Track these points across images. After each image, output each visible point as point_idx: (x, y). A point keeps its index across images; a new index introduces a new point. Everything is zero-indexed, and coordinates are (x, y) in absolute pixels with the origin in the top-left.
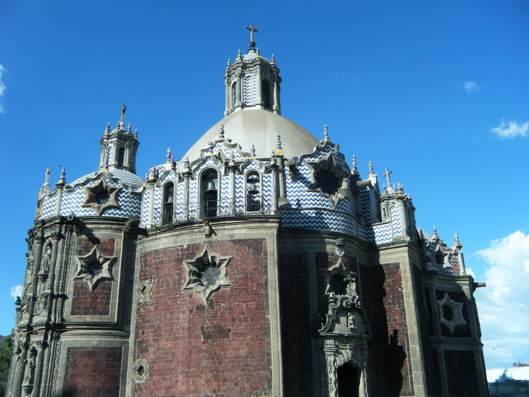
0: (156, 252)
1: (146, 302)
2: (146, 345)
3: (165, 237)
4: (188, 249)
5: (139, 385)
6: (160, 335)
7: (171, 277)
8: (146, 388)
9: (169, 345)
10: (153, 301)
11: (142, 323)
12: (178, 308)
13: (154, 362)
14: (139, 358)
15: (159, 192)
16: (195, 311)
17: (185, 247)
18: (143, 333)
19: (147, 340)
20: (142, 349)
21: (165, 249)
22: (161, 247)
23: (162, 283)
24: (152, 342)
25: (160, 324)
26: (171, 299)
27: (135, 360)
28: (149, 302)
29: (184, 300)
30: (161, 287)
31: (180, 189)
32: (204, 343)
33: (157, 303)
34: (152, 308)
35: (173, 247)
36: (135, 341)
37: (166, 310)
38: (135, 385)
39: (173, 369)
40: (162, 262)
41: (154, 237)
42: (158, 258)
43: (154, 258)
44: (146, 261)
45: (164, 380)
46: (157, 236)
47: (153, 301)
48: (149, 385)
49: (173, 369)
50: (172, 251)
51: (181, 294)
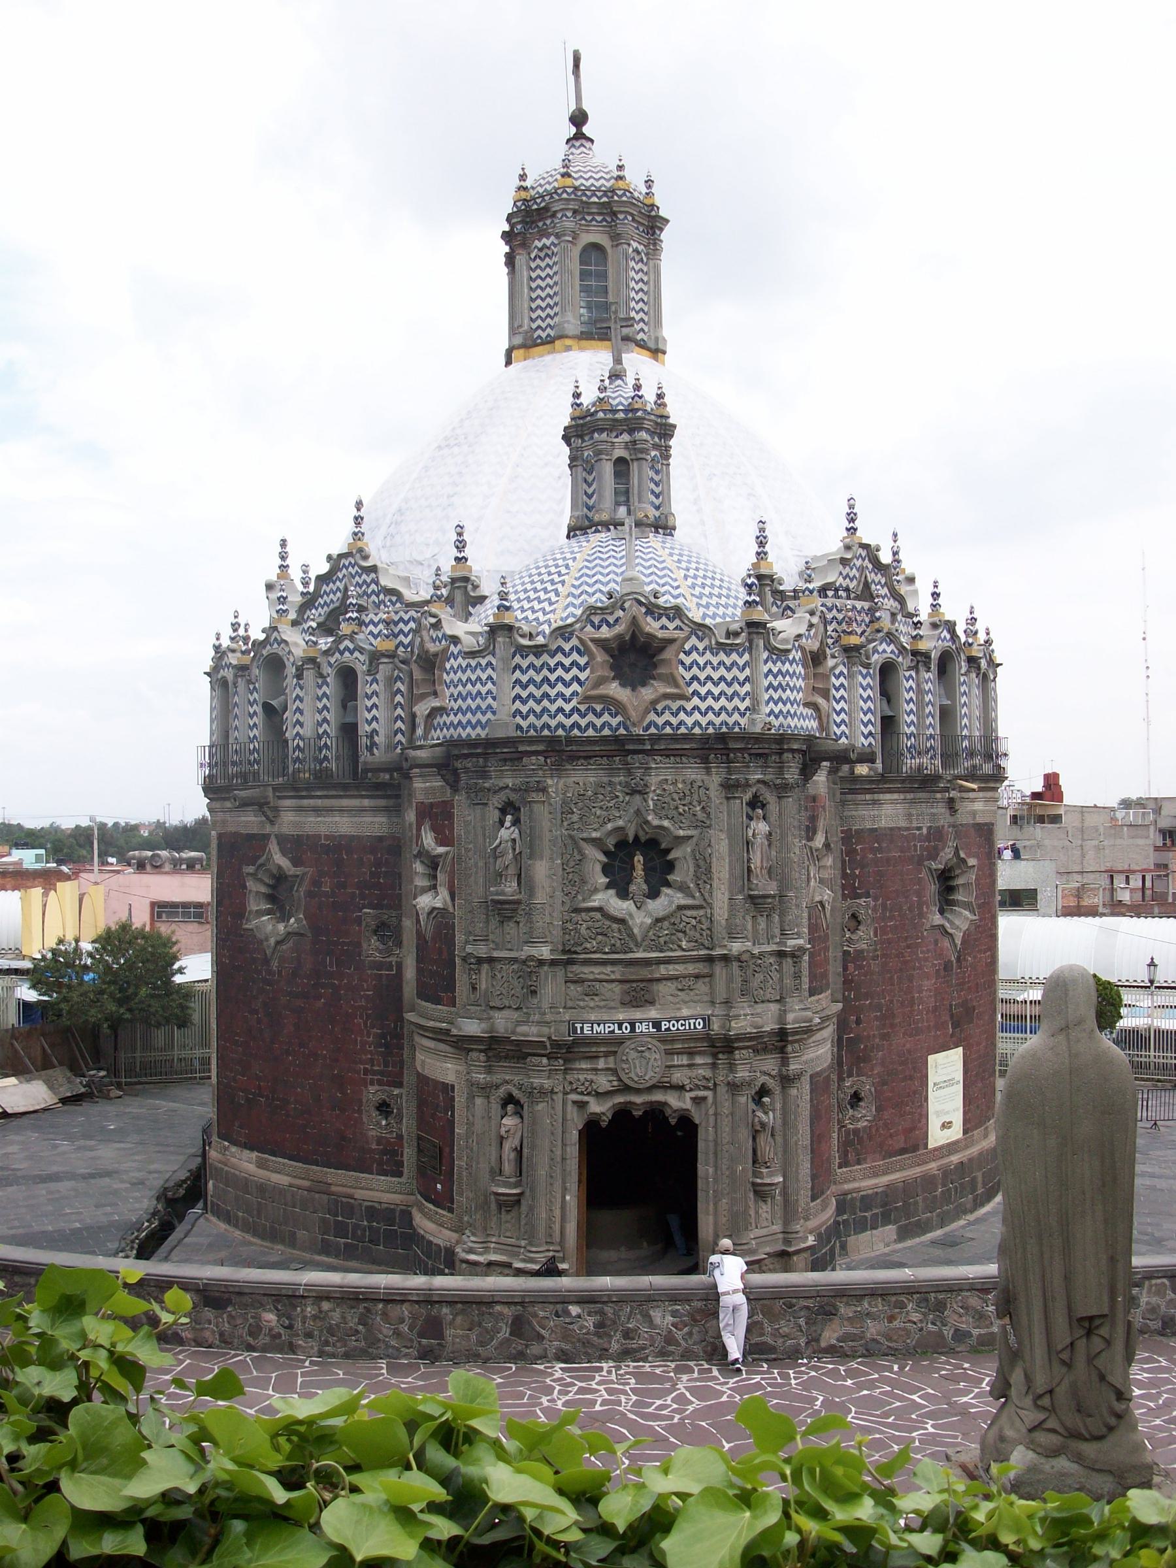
0: (875, 834)
1: (862, 951)
2: (866, 1046)
3: (893, 802)
4: (928, 838)
5: (856, 1132)
6: (892, 1026)
7: (906, 897)
8: (870, 1138)
9: (908, 1046)
10: (876, 950)
11: (855, 999)
12: (920, 968)
13: (884, 1083)
14: (849, 1076)
15: (866, 685)
16: (942, 973)
17: (925, 831)
18: (858, 1022)
19: (869, 1036)
20: (859, 1057)
21: (891, 829)
22: (883, 824)
23: (891, 911)
24: (877, 1040)
25: (891, 1001)
26: (908, 947)
27: (841, 1079)
28: (868, 952)
29: (928, 951)
30: (891, 918)
31: (906, 684)
32: (952, 1036)
33: (883, 955)
34: (875, 966)
35: (908, 829)
36: (840, 1039)
37: (901, 970)
38: (848, 1132)
39: (915, 1093)
40: (888, 860)
41: (868, 797)
42: (880, 850)
43: (874, 851)
44: (851, 852)
45: (902, 1116)
46: (876, 796)
47: (876, 950)
48: (877, 1130)
49: (915, 1093)
50: (906, 837)
51: (922, 937)
